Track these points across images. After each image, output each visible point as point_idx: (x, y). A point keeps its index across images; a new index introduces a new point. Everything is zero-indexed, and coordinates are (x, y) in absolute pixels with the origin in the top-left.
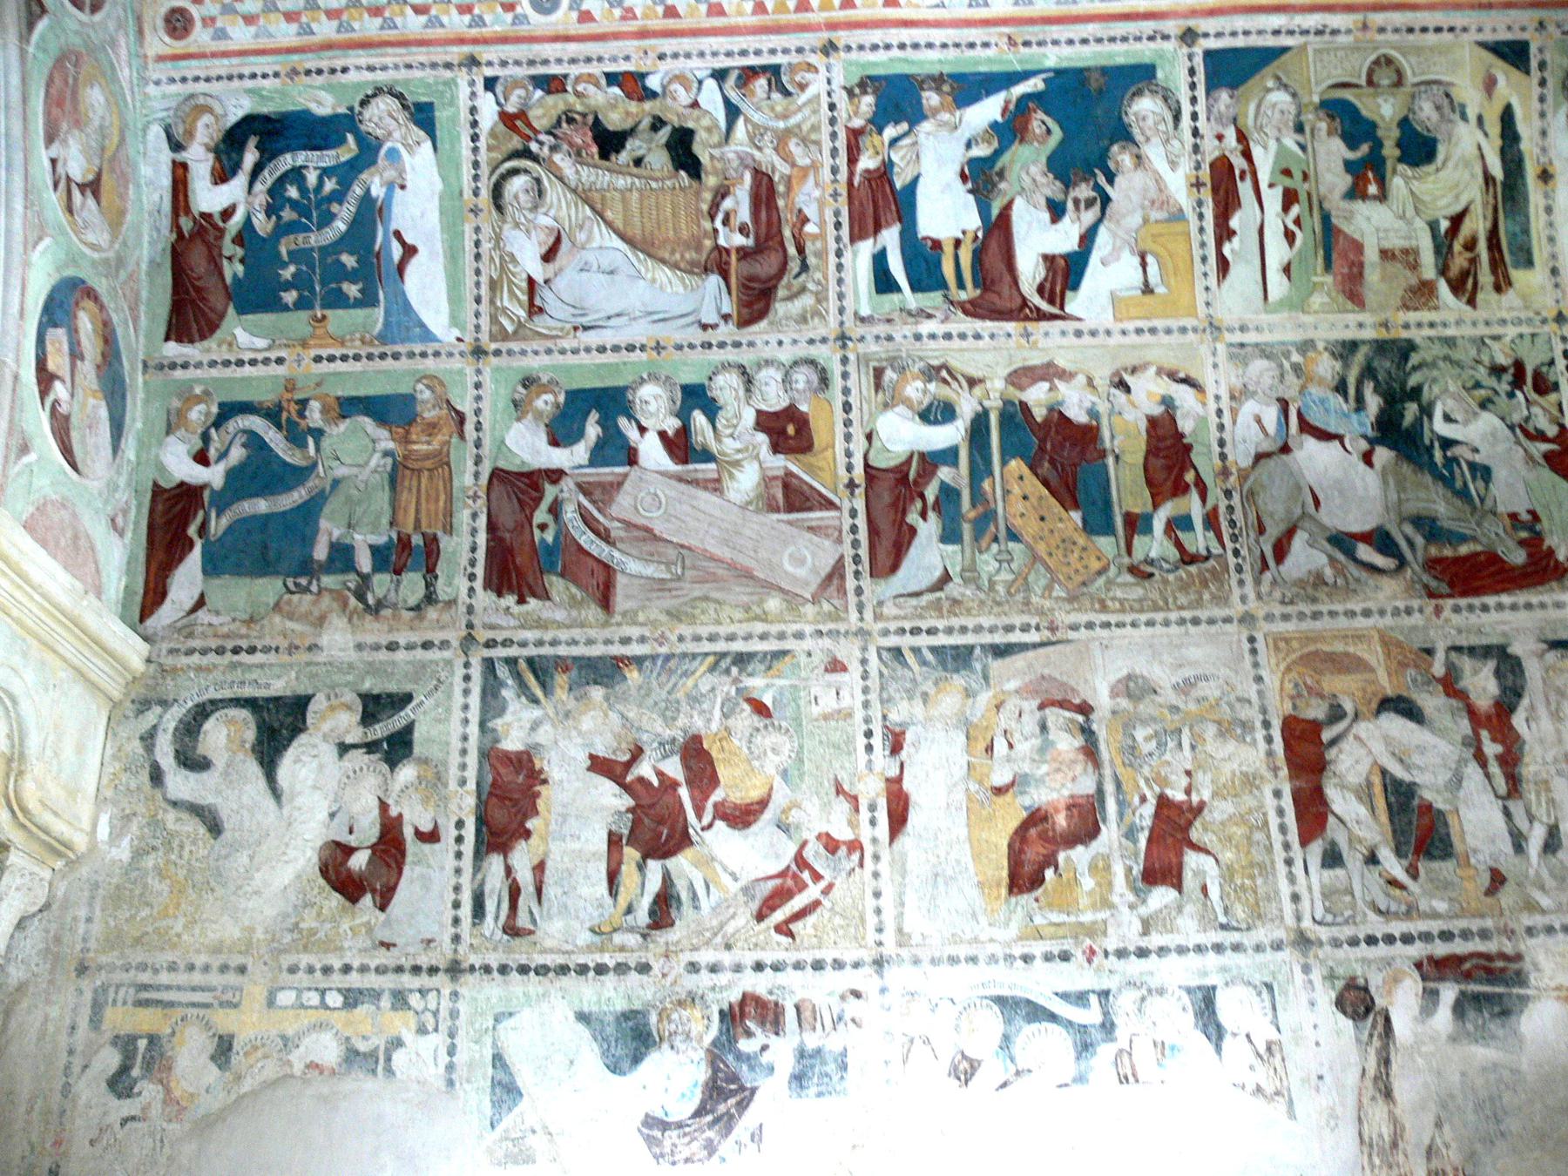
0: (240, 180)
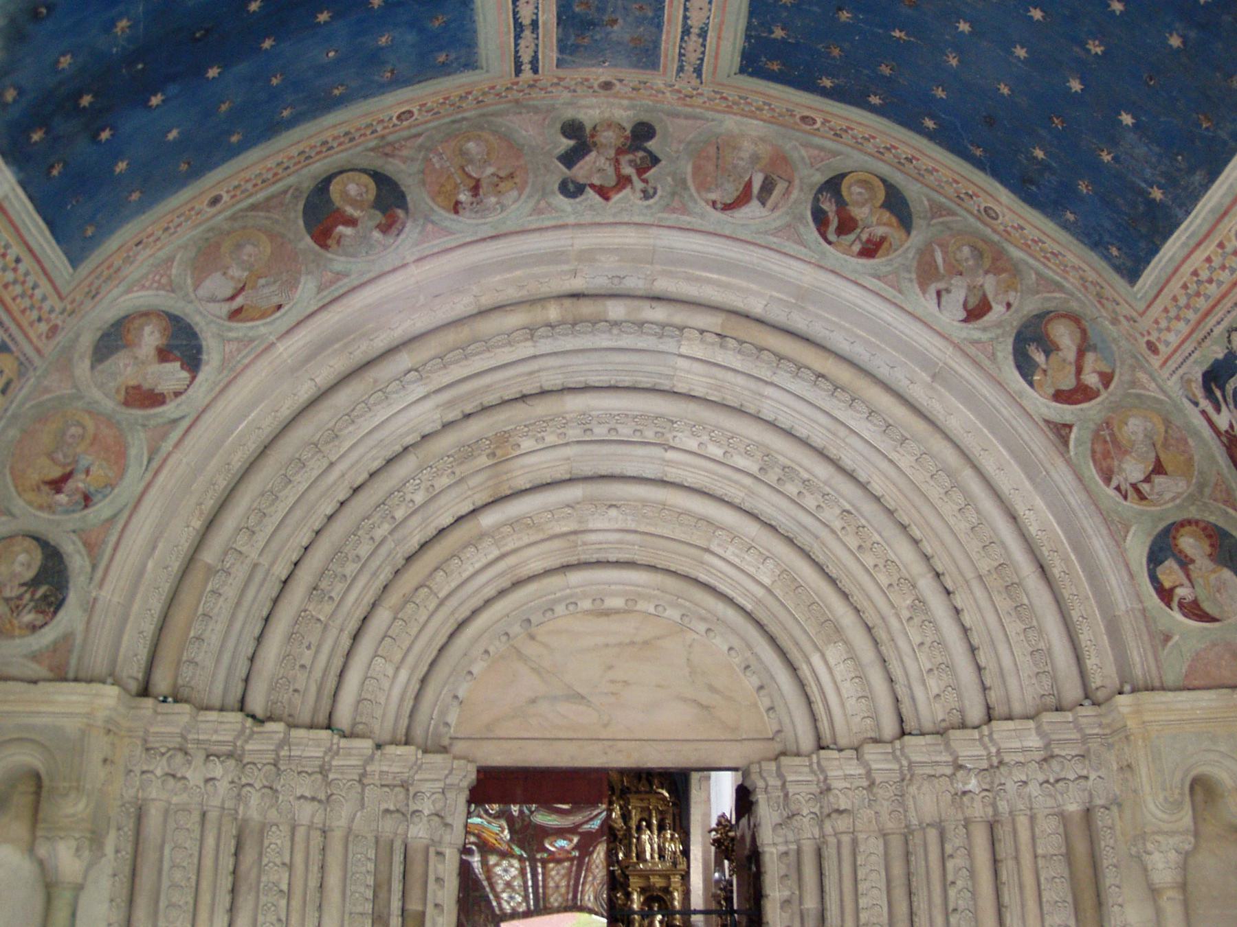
0: (1224, 407)
